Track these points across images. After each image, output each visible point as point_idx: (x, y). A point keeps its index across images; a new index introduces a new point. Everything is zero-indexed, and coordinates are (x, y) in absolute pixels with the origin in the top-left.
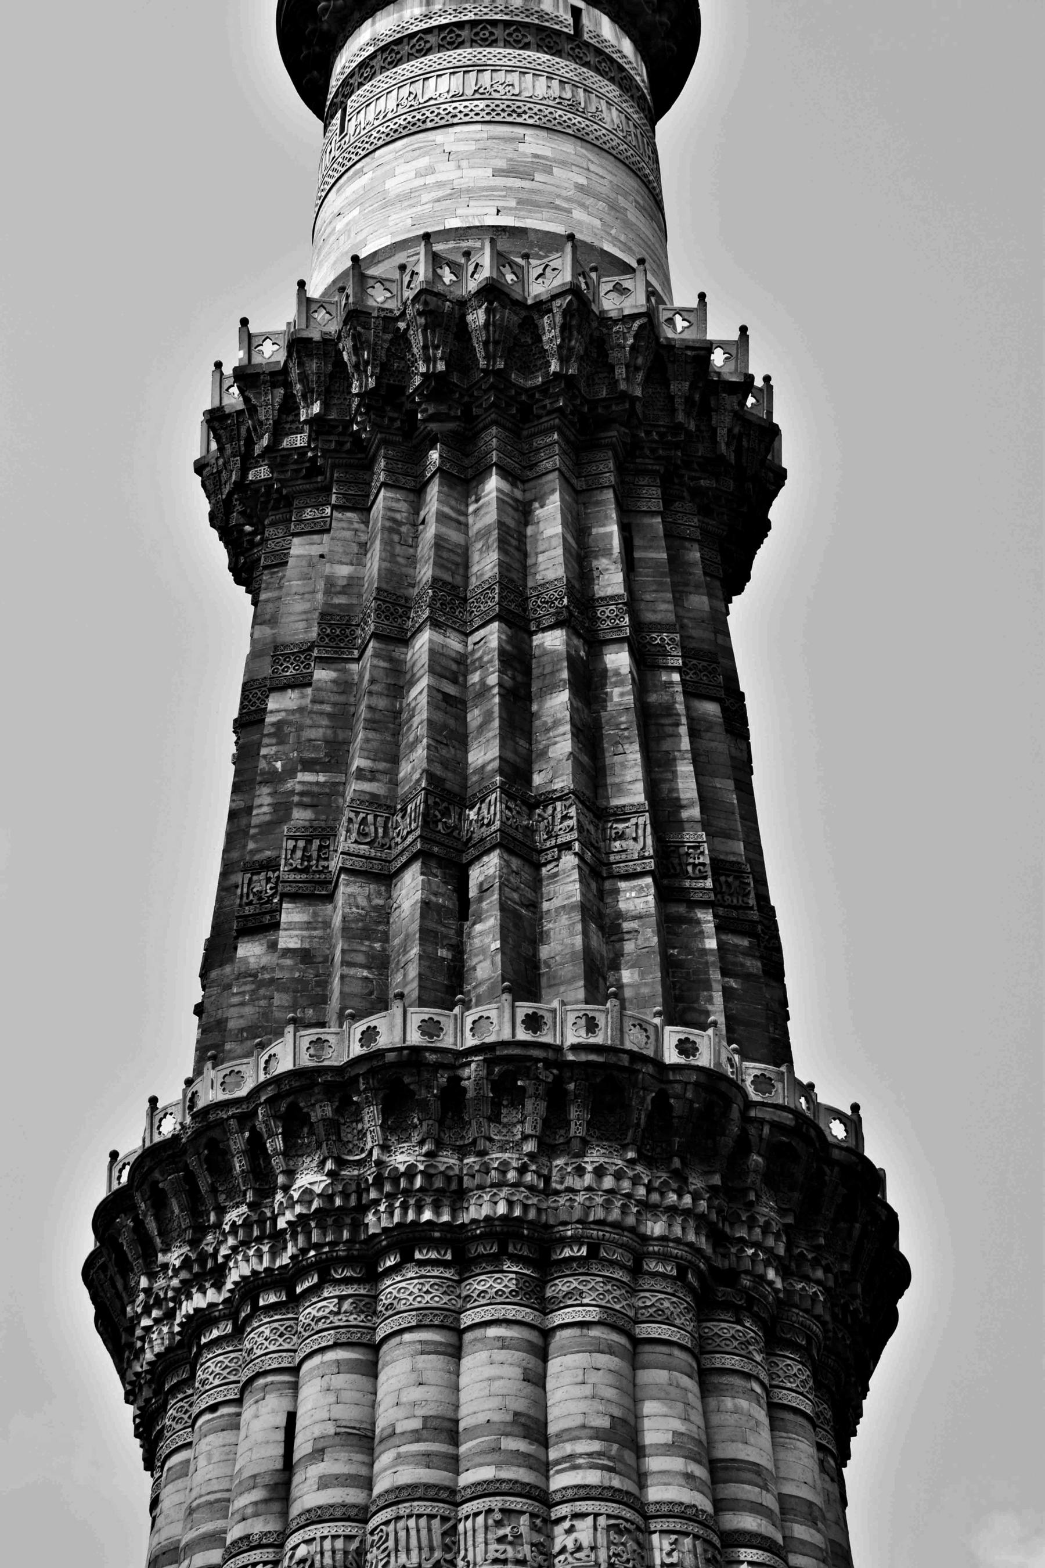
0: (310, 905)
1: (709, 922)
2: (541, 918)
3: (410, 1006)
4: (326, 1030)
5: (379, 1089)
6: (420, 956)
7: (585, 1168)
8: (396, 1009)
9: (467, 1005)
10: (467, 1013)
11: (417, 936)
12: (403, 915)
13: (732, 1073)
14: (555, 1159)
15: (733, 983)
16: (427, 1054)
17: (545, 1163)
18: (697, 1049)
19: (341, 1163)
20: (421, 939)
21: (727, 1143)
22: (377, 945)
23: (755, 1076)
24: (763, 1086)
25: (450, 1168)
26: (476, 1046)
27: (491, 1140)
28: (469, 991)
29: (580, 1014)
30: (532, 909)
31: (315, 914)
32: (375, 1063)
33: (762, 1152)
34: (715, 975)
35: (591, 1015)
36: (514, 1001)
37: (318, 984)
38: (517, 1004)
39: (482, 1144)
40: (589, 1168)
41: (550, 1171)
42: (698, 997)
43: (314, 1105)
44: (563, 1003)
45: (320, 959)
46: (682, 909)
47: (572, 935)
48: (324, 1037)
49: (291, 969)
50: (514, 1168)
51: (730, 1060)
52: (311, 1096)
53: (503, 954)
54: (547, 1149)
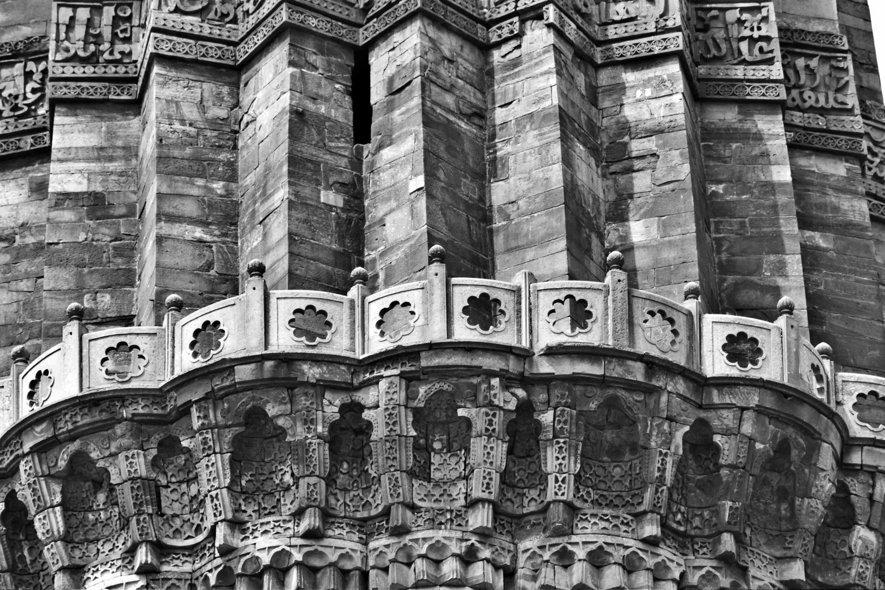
0: (102, 119)
1: (778, 136)
2: (493, 136)
3: (275, 287)
4: (134, 329)
5: (227, 427)
6: (290, 202)
7: (572, 554)
8: (252, 291)
9: (370, 284)
10: (370, 298)
11: (285, 168)
12: (261, 134)
13: (820, 390)
14: (522, 539)
15: (819, 240)
16: (305, 367)
17: (506, 545)
18: (759, 352)
19: (161, 550)
20: (290, 174)
21: (814, 508)
22: (218, 186)
23: (861, 396)
24: (874, 411)
25: (345, 556)
26: (387, 352)
27: (413, 508)
28: (374, 261)
29: (562, 295)
30: (476, 121)
31: (111, 134)
32: (218, 383)
33: (875, 524)
34: (789, 226)
35: (578, 296)
36: (449, 275)
37: (119, 252)
38: (454, 280)
39: (399, 516)
40: (581, 553)
41: (515, 559)
42: (759, 266)
43: (114, 455)
44: (532, 278)
45: (122, 211)
46: (729, 116)
47: (545, 163)
48: (130, 341)
49: (72, 227)
50: (454, 555)
51: (815, 369)
52: (110, 439)
53: (430, 196)
54: (508, 522)
